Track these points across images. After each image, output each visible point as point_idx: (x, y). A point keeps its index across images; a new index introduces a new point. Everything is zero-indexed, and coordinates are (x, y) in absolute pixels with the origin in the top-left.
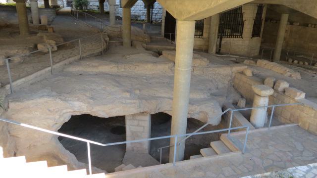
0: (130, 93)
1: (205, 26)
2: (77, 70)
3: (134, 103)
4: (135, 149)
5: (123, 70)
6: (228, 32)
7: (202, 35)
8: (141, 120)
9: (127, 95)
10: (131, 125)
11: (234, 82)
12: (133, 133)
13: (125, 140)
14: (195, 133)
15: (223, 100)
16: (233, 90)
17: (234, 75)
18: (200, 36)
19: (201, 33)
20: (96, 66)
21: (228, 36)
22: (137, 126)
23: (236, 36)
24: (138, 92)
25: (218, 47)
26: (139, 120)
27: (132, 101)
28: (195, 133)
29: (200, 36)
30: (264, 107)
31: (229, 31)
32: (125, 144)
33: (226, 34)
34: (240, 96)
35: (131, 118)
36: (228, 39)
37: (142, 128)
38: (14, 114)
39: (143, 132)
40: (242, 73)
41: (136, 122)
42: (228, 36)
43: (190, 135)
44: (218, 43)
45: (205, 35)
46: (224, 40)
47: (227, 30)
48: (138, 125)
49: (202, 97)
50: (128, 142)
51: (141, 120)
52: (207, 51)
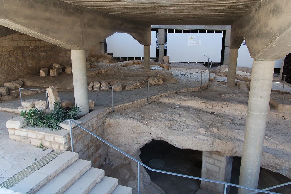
0: (207, 129)
2: (169, 102)
3: (207, 140)
8: (218, 160)
9: (203, 131)
10: (207, 163)
12: (208, 170)
13: (200, 177)
14: (264, 191)
24: (215, 130)
26: (215, 159)
27: (206, 138)
35: (208, 155)
37: (218, 168)
38: (108, 128)
39: (218, 173)
41: (212, 161)
51: (218, 160)
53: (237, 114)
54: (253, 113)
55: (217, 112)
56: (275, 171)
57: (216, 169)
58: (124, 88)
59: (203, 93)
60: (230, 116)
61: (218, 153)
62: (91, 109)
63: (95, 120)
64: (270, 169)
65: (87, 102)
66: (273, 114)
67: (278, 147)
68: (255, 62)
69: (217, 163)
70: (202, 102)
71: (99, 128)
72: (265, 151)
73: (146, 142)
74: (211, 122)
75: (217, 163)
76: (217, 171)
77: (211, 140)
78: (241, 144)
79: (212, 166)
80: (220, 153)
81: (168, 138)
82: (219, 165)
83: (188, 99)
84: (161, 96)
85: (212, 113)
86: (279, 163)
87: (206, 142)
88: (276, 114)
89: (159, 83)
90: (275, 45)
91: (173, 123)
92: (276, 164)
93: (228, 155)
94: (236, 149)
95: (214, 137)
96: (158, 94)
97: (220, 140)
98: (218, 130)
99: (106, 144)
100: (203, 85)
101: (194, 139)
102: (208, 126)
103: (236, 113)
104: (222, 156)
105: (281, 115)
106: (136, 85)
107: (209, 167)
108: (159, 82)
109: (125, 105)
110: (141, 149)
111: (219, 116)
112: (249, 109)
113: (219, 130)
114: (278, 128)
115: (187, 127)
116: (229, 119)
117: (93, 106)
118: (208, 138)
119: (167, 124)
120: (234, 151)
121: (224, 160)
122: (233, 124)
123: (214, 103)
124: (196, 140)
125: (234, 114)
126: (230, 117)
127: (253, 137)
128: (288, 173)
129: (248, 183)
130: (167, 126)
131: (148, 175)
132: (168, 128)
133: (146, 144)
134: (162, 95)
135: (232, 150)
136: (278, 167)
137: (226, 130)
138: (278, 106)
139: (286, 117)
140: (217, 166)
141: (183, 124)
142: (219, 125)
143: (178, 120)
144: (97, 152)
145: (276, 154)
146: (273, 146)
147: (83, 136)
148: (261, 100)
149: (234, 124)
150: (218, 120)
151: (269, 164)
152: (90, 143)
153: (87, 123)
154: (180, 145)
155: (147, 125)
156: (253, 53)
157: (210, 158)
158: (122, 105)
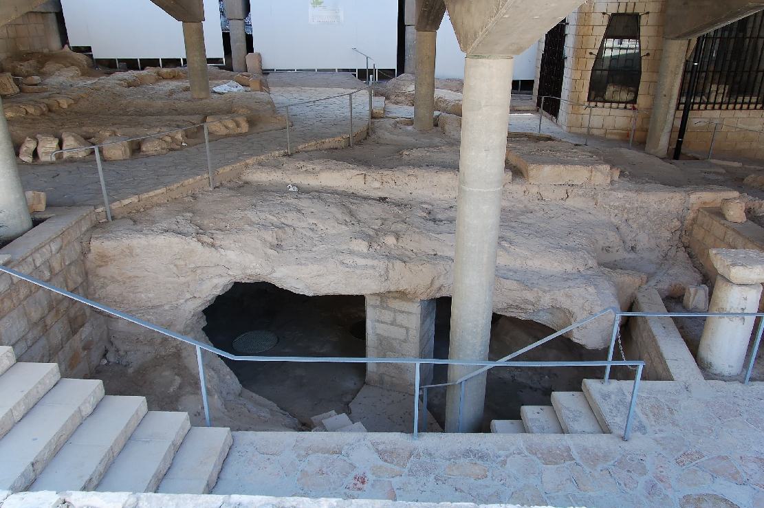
0: (370, 240)
1: (644, 77)
3: (373, 267)
4: (387, 378)
5: (377, 185)
6: (717, 91)
7: (634, 101)
9: (361, 246)
11: (691, 234)
12: (381, 339)
13: (363, 355)
14: (502, 362)
15: (630, 281)
16: (682, 255)
17: (691, 215)
18: (626, 103)
19: (631, 97)
20: (314, 173)
21: (715, 103)
22: (392, 324)
23: (743, 103)
24: (390, 240)
25: (676, 135)
26: (395, 311)
27: (370, 262)
28: (502, 362)
29: (626, 103)
30: (742, 314)
31: (721, 91)
32: (365, 364)
33: (712, 100)
34: (699, 277)
35: (378, 303)
36: (717, 113)
37: (403, 331)
38: (101, 266)
39: (405, 341)
40: (719, 213)
41: (387, 316)
42: (715, 103)
43: (491, 365)
44: (678, 123)
45: (642, 101)
46: (700, 118)
47: (714, 87)
48: (393, 323)
49: (569, 267)
50: (371, 360)
52: (641, 144)
53: (441, 197)
54: (471, 189)
55: (392, 196)
56: (523, 317)
57: (398, 333)
58: (136, 148)
59: (358, 151)
60: (425, 203)
61: (402, 295)
62: (37, 216)
63: (54, 247)
64: (513, 315)
65: (18, 196)
66: (517, 188)
67: (530, 263)
68: (473, 61)
69: (401, 319)
70: (355, 172)
71: (73, 268)
72: (500, 274)
73: (218, 292)
74: (379, 222)
75: (401, 319)
76: (402, 338)
77: (381, 264)
79: (389, 327)
80: (406, 294)
81: (274, 275)
82: (405, 323)
83: (318, 168)
84: (247, 166)
85: (383, 200)
86: (533, 300)
87: (371, 271)
88: (524, 189)
89: (239, 130)
90: (507, 16)
91: (285, 233)
92: (526, 301)
93: (424, 297)
94: (441, 281)
95: (389, 257)
96: (237, 160)
97: (404, 262)
98: (397, 239)
99: (101, 313)
100: (355, 131)
101: (341, 267)
102: (371, 233)
103: (437, 196)
104: (411, 300)
105: (534, 190)
106: (172, 138)
107: (383, 330)
108: (238, 125)
109: (145, 196)
110: (205, 311)
111: (398, 205)
112: (462, 182)
113: (400, 240)
114: (529, 221)
115: (322, 240)
116: (423, 210)
117: (42, 207)
118: (375, 263)
119: (270, 239)
120: (437, 285)
121: (415, 308)
122: (430, 222)
123: (386, 173)
124: (348, 269)
125: (433, 196)
126: (424, 206)
127: (473, 245)
128: (550, 316)
129: (468, 352)
130: (270, 243)
131: (233, 375)
132: (272, 247)
133: (219, 298)
134: (249, 161)
135: (432, 283)
136: (530, 307)
137: (417, 237)
138: (527, 171)
139: (545, 194)
140: (401, 326)
141: (310, 234)
142: (400, 226)
143: (296, 224)
144: (77, 337)
145: (526, 279)
146: (517, 264)
147: (22, 297)
148: (487, 156)
149: (434, 220)
150: (396, 215)
151: (511, 302)
152: (47, 315)
153: (30, 259)
154: (308, 287)
155: (213, 245)
156: (464, 39)
157: (384, 308)
158: (134, 199)
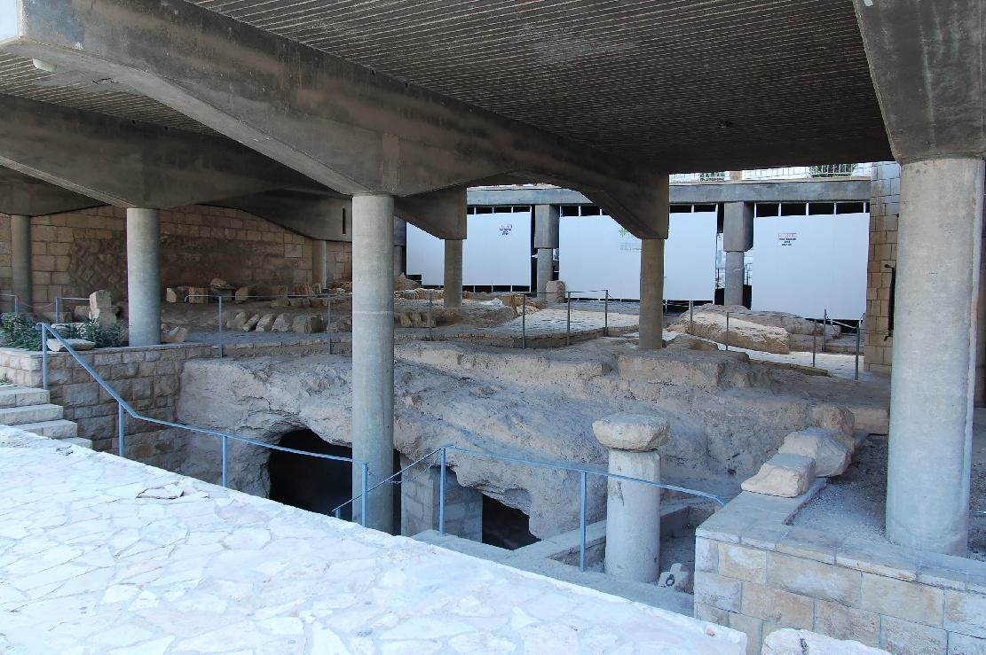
78: (441, 430)
155: (265, 381)
